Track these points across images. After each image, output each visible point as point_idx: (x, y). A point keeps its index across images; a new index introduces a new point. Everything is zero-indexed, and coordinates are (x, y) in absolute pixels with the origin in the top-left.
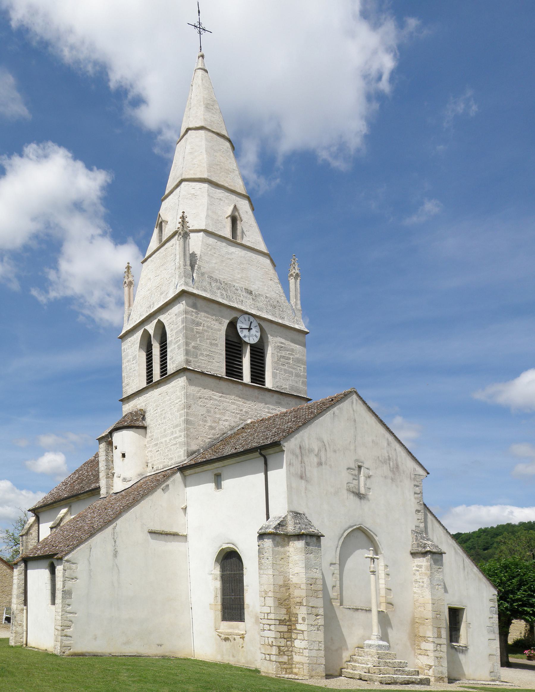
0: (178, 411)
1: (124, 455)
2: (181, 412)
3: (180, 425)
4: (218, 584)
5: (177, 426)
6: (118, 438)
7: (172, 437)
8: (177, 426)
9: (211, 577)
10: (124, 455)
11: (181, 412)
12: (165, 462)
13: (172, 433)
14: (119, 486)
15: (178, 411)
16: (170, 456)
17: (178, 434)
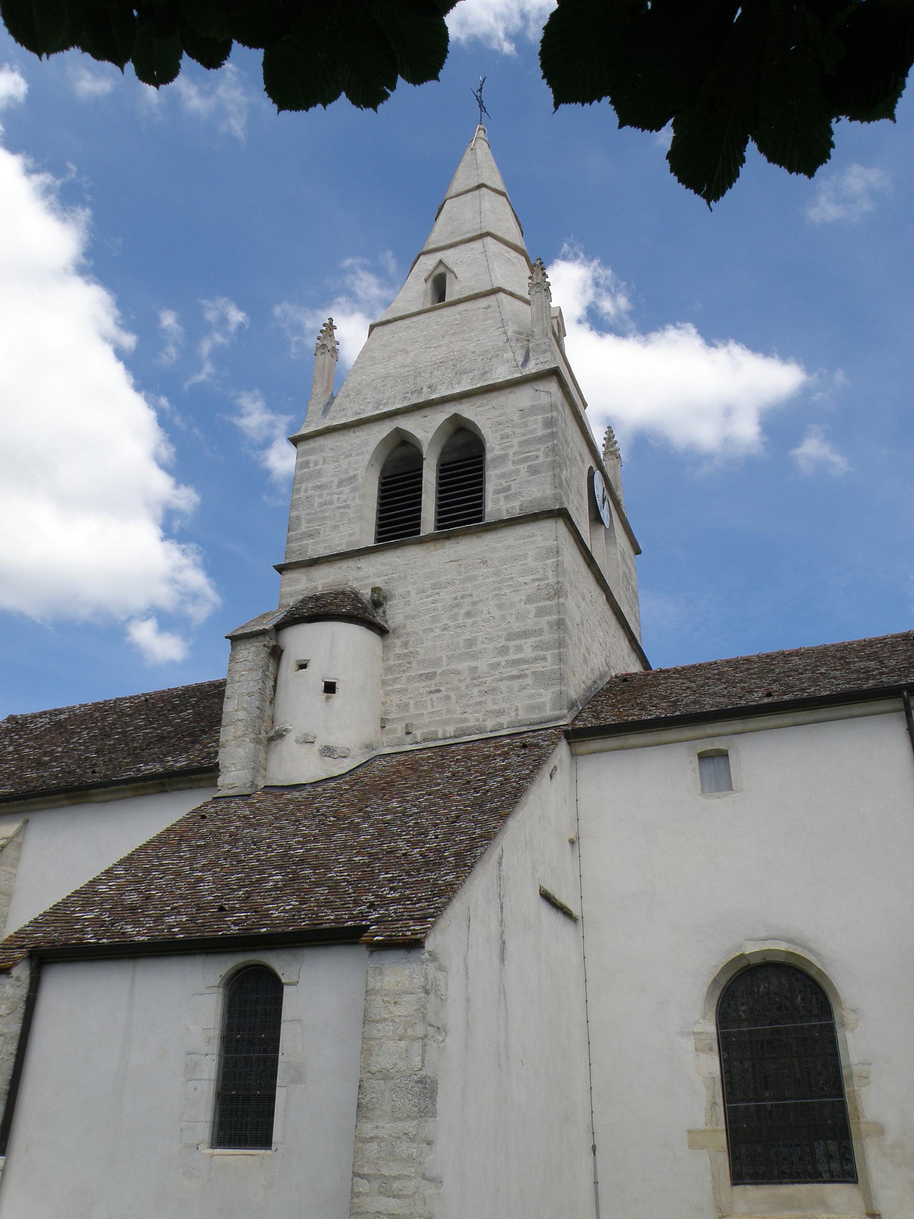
0: (530, 600)
1: (330, 688)
2: (542, 604)
3: (539, 632)
4: (712, 1064)
5: (525, 634)
6: (302, 640)
7: (502, 660)
8: (525, 634)
9: (689, 1044)
10: (330, 688)
11: (542, 604)
12: (466, 720)
13: (504, 650)
14: (298, 765)
15: (530, 600)
16: (490, 706)
17: (528, 652)
